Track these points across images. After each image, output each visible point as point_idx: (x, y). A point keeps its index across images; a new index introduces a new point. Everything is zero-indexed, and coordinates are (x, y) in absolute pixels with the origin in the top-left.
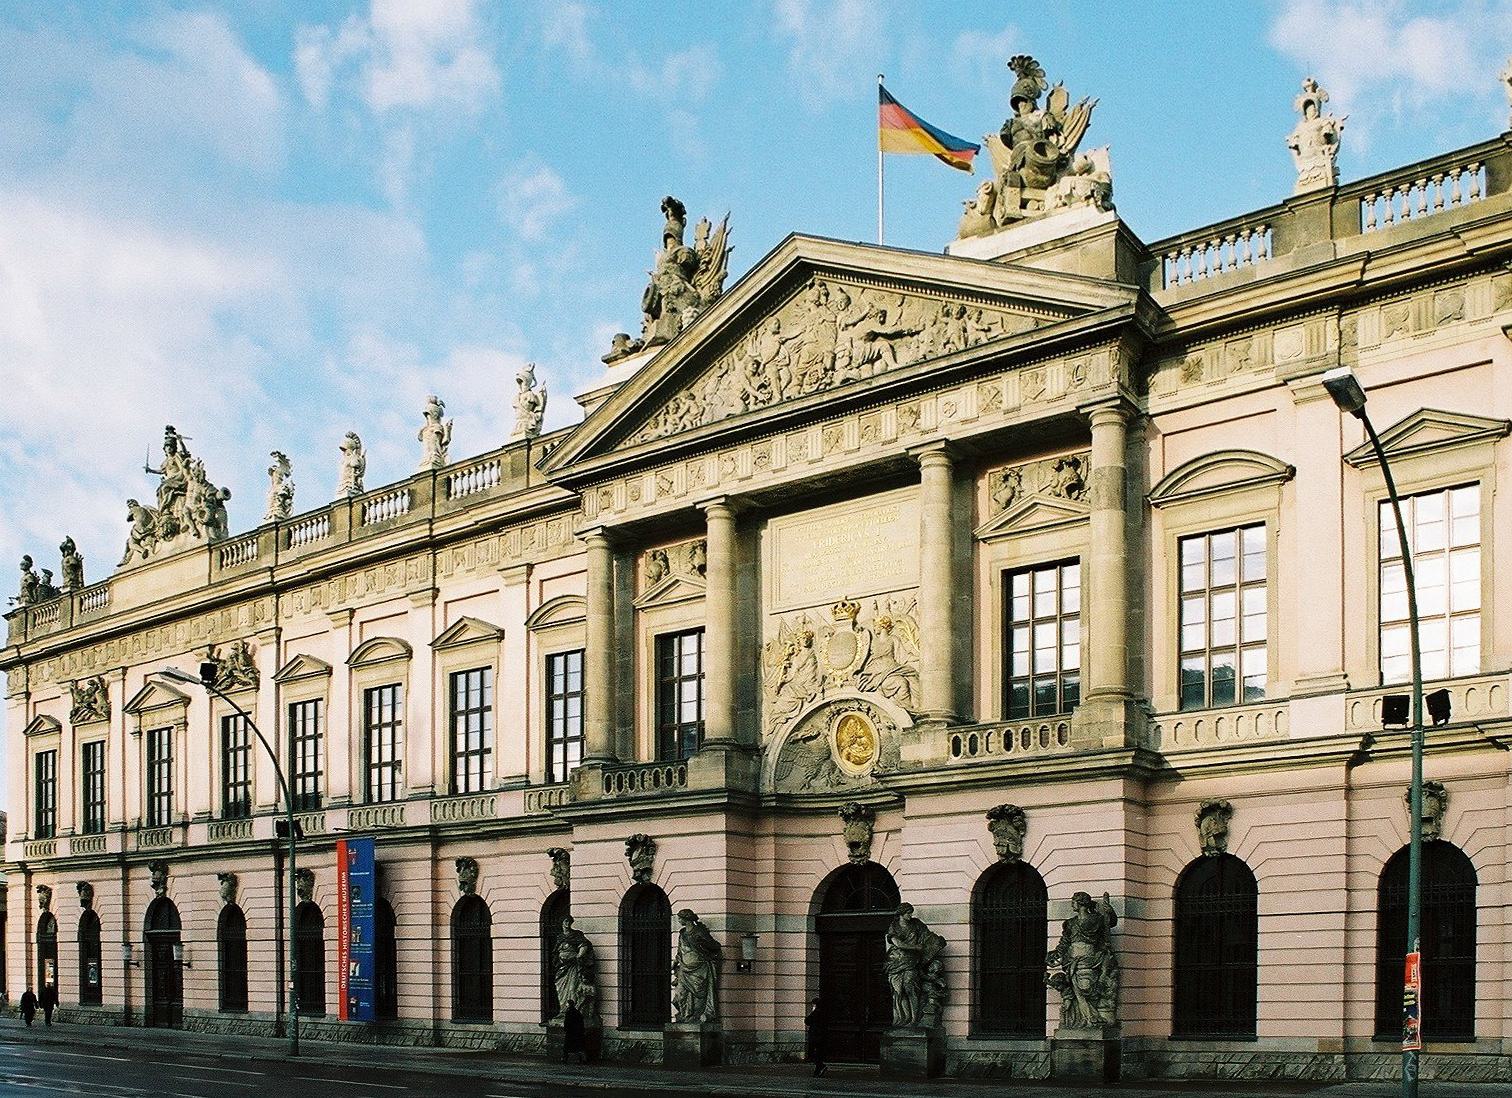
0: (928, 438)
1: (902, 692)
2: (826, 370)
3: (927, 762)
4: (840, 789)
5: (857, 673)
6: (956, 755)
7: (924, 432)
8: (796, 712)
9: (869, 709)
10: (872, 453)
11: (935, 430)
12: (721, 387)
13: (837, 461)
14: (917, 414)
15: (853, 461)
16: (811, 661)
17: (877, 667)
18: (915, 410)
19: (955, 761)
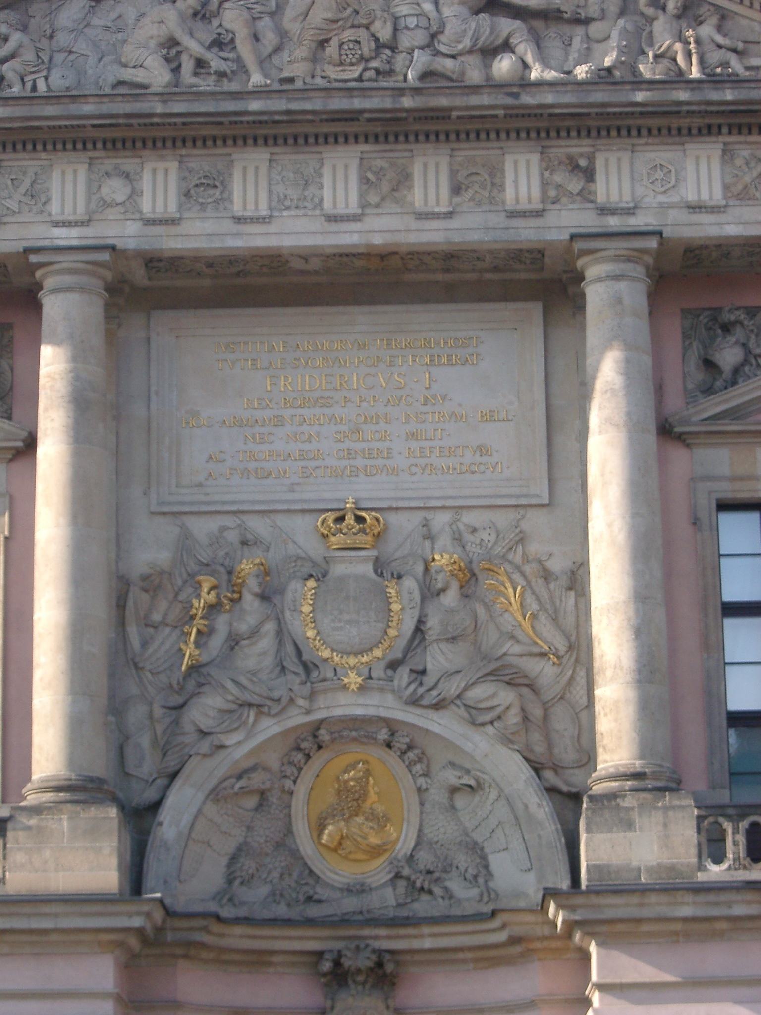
0: (614, 222)
1: (513, 718)
2: (379, 46)
3: (650, 870)
4: (313, 911)
5: (393, 665)
6: (718, 860)
7: (604, 210)
8: (231, 740)
9: (410, 747)
10: (472, 227)
11: (629, 212)
12: (96, 21)
13: (384, 229)
14: (589, 174)
15: (433, 235)
16: (270, 627)
17: (437, 658)
18: (583, 162)
19: (715, 871)
